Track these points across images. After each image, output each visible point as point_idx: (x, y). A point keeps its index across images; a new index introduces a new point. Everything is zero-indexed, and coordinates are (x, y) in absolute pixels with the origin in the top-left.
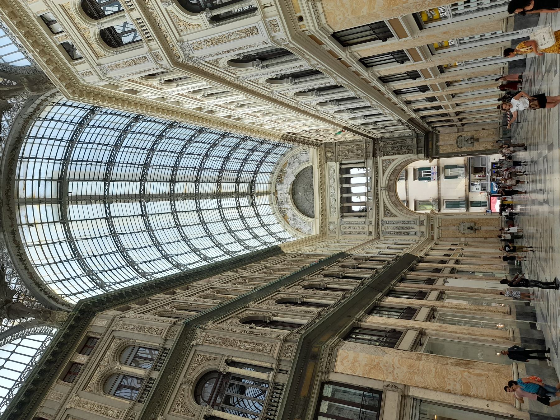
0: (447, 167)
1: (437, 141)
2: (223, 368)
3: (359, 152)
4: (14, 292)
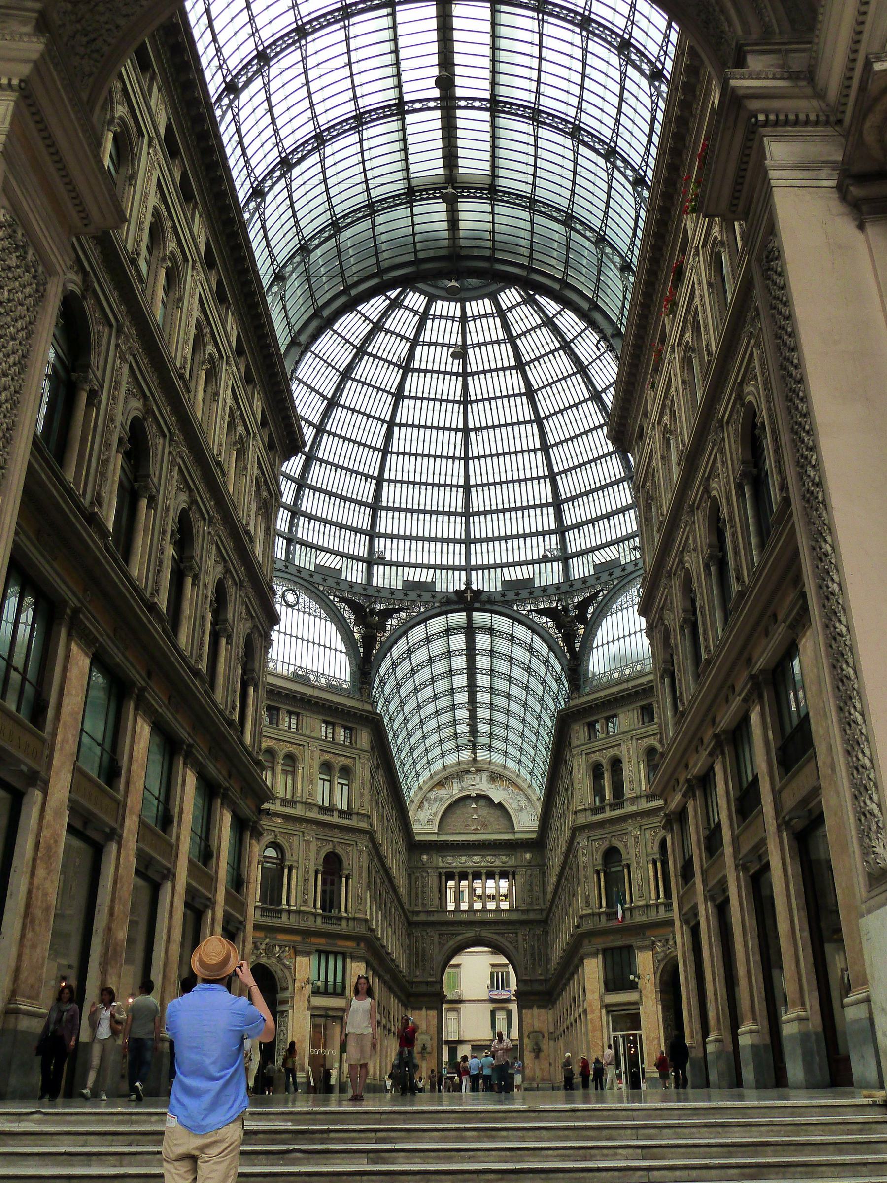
0: (509, 1014)
1: (539, 1007)
2: (346, 872)
3: (529, 900)
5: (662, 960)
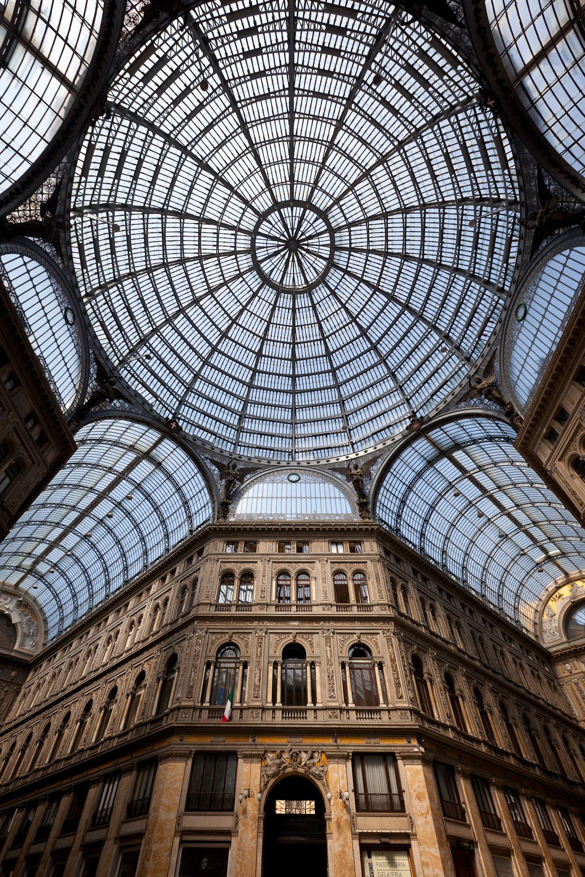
4: (111, 401)
5: (273, 776)
